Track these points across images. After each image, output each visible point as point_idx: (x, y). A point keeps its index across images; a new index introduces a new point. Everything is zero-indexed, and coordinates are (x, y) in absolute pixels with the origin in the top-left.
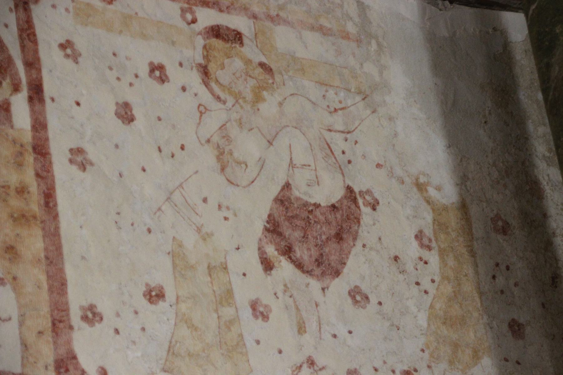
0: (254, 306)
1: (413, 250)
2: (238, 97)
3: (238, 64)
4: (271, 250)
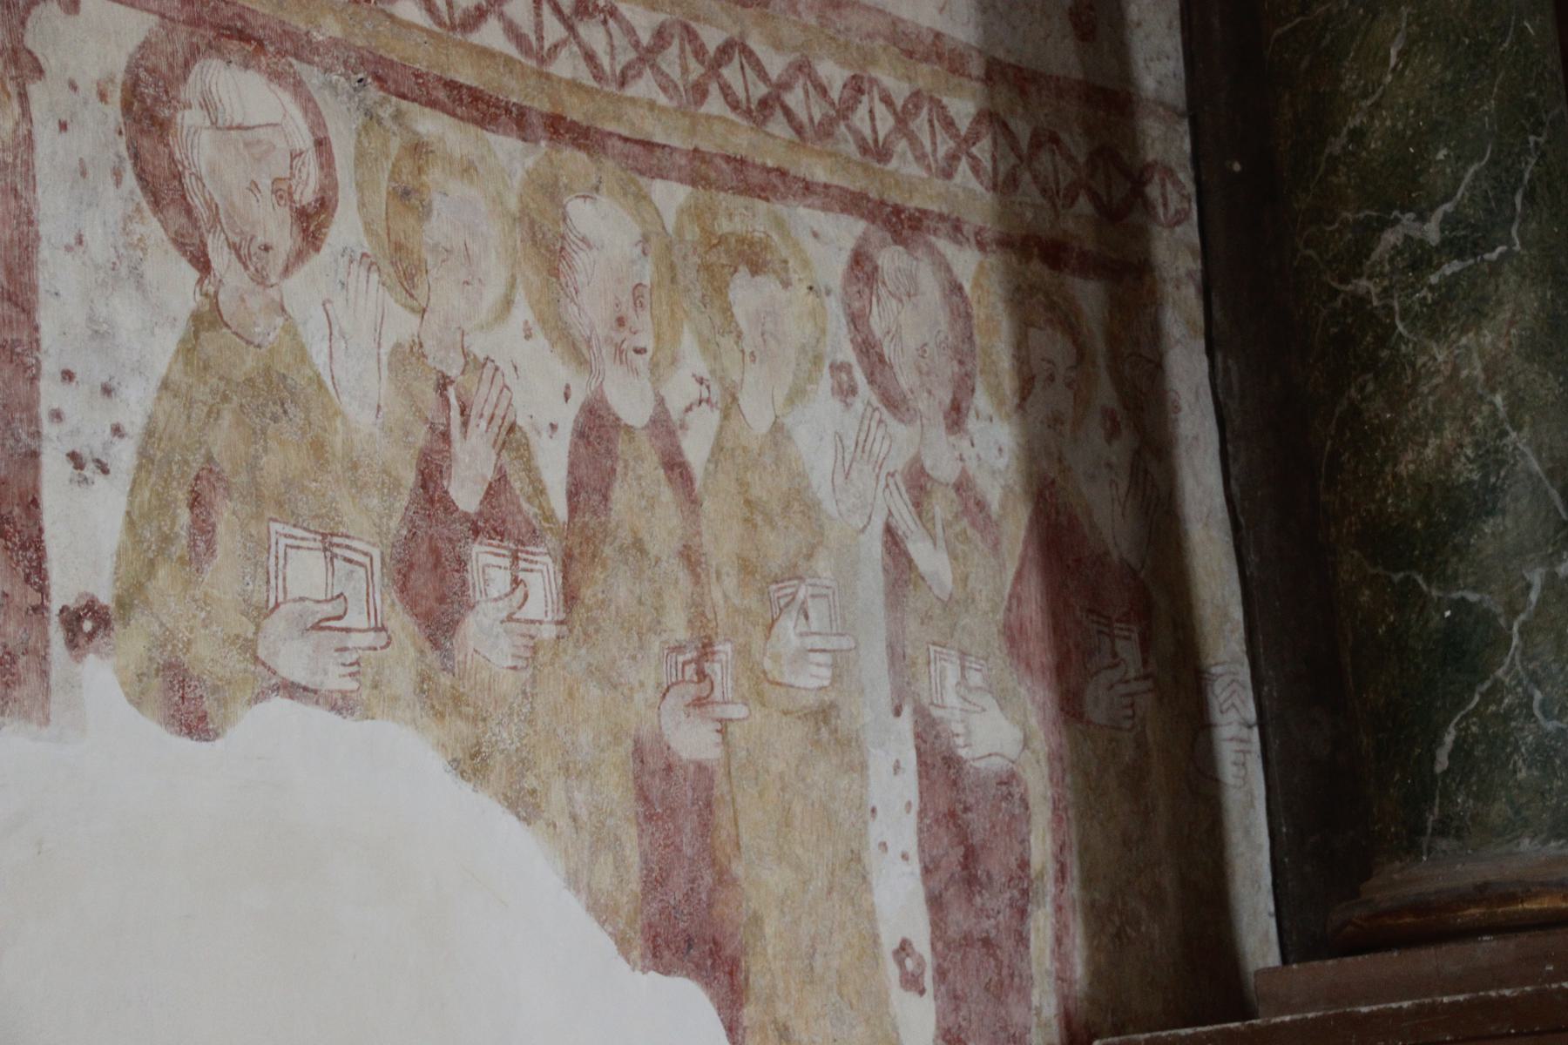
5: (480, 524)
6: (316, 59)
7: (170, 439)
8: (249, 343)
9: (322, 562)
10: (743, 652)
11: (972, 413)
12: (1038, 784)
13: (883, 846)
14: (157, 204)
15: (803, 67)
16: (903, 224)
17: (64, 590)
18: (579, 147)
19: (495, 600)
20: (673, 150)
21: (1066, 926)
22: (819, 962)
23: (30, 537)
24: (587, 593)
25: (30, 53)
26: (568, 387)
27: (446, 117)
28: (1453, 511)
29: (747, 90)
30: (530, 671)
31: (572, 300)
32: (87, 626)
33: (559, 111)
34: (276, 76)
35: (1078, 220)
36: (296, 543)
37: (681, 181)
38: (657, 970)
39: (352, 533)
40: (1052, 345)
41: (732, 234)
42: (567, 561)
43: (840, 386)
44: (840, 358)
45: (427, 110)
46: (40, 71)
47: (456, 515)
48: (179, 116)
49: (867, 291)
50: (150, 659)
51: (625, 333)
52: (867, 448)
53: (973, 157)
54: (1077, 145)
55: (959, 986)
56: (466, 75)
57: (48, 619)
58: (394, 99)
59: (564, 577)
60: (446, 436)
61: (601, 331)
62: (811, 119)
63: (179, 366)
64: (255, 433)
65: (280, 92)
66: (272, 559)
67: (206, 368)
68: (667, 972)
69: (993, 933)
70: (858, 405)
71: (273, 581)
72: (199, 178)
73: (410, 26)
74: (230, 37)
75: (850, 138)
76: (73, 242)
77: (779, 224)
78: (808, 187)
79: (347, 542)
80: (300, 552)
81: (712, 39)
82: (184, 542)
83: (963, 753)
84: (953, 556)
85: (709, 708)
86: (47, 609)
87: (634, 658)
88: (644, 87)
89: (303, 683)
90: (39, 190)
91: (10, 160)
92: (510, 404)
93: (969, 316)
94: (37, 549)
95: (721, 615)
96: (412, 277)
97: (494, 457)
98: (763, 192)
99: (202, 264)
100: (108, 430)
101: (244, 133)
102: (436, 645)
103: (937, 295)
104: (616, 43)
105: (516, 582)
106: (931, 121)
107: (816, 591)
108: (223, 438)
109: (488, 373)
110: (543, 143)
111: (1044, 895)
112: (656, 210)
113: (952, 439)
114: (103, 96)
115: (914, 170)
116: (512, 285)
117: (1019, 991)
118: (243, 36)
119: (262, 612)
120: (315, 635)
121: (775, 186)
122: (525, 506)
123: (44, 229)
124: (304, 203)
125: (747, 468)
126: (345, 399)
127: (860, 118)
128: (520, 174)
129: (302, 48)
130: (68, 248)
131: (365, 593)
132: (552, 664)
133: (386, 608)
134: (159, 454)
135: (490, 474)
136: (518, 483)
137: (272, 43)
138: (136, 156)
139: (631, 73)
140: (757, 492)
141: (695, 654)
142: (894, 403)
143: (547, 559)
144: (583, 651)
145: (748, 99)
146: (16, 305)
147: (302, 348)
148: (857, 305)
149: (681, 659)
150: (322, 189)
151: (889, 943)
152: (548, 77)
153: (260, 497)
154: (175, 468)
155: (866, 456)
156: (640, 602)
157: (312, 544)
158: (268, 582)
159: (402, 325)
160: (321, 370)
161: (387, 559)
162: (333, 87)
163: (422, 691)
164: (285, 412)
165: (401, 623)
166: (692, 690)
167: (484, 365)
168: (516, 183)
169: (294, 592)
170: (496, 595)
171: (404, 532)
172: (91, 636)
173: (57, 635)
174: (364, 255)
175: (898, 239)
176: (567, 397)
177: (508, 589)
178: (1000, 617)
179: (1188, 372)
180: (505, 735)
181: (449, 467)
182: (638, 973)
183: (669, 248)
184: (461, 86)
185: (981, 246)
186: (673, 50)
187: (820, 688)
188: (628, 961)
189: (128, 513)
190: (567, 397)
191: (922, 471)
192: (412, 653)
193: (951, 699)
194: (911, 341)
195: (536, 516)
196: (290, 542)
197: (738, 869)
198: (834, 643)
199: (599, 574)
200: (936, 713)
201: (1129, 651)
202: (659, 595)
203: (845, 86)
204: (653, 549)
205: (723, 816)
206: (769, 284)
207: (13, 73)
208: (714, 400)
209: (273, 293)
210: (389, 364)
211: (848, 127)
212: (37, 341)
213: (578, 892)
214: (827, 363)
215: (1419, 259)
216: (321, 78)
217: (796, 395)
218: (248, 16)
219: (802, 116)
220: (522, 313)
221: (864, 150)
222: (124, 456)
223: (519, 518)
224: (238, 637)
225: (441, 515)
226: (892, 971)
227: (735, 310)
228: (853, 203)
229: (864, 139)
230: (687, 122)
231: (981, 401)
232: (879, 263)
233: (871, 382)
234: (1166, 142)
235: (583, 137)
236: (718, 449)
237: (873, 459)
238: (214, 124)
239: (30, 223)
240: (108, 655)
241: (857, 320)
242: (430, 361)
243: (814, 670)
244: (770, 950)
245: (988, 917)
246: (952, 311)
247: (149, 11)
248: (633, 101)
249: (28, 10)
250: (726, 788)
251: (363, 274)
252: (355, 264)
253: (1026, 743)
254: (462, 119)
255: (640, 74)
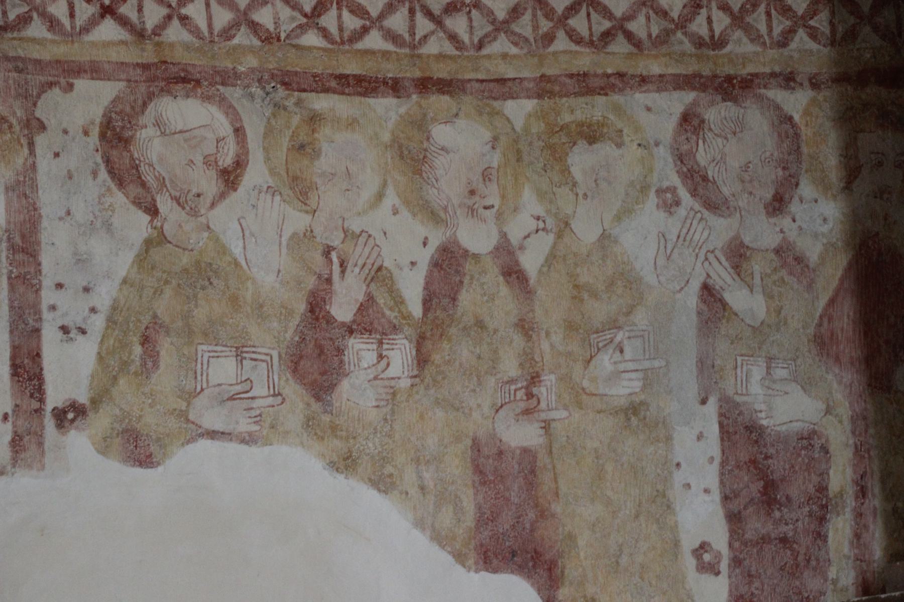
5: (354, 327)
6: (239, 82)
7: (128, 309)
8: (184, 249)
9: (234, 363)
10: (565, 379)
11: (796, 199)
13: (688, 486)
14: (121, 184)
17: (55, 397)
18: (444, 93)
19: (366, 369)
20: (521, 80)
21: (866, 527)
22: (624, 560)
23: (35, 374)
24: (436, 358)
25: (38, 119)
26: (426, 238)
27: (336, 97)
29: (590, 29)
30: (390, 407)
31: (433, 186)
32: (70, 416)
33: (427, 74)
34: (207, 98)
36: (216, 354)
37: (529, 97)
38: (487, 570)
39: (257, 344)
41: (573, 122)
42: (420, 342)
43: (665, 202)
44: (665, 184)
45: (322, 95)
46: (43, 127)
47: (335, 324)
48: (138, 133)
49: (694, 137)
50: (112, 429)
51: (477, 198)
52: (688, 239)
53: (811, 27)
55: (753, 569)
56: (352, 68)
57: (44, 415)
58: (296, 93)
59: (417, 350)
60: (329, 281)
61: (456, 201)
62: (650, 36)
63: (135, 269)
64: (188, 298)
65: (209, 107)
66: (199, 366)
67: (152, 268)
68: (495, 571)
69: (791, 534)
70: (682, 212)
71: (199, 378)
72: (151, 165)
73: (310, 49)
74: (176, 83)
75: (686, 40)
76: (63, 215)
77: (618, 109)
78: (644, 80)
79: (254, 349)
80: (219, 359)
82: (138, 364)
83: (764, 422)
84: (769, 296)
85: (536, 415)
86: (43, 410)
87: (474, 391)
89: (221, 430)
90: (40, 192)
91: (22, 179)
92: (379, 255)
93: (797, 135)
94: (39, 379)
95: (547, 357)
96: (306, 193)
97: (364, 288)
99: (153, 211)
100: (87, 310)
101: (184, 135)
102: (318, 398)
103: (766, 128)
104: (475, 24)
105: (381, 357)
106: (768, 14)
107: (632, 334)
108: (165, 305)
109: (362, 240)
110: (414, 97)
111: (844, 507)
112: (508, 119)
113: (772, 220)
114: (86, 133)
115: (749, 48)
116: (385, 185)
117: (815, 569)
118: (185, 80)
119: (191, 396)
120: (230, 403)
121: (613, 85)
122: (388, 313)
123: (43, 212)
124: (225, 166)
125: (576, 265)
126: (254, 270)
127: (699, 26)
128: (394, 117)
129: (227, 78)
130: (61, 219)
131: (265, 376)
132: (408, 401)
133: (282, 383)
134: (121, 319)
135: (361, 298)
136: (382, 299)
137: (206, 80)
138: (108, 161)
139: (486, 40)
140: (585, 277)
141: (525, 384)
143: (405, 342)
144: (432, 391)
145: (591, 35)
146: (27, 254)
147: (223, 246)
148: (685, 148)
149: (513, 387)
150: (238, 156)
151: (688, 543)
152: (419, 56)
153: (191, 333)
154: (131, 325)
155: (687, 243)
156: (479, 357)
157: (228, 354)
158: (196, 378)
159: (298, 221)
160: (237, 256)
161: (284, 356)
162: (252, 96)
163: (308, 426)
164: (211, 283)
165: (293, 390)
166: (522, 405)
167: (360, 235)
168: (390, 125)
169: (214, 380)
170: (366, 366)
171: (297, 339)
172: (73, 421)
173: (49, 423)
174: (269, 187)
175: (728, 96)
176: (425, 244)
177: (375, 361)
178: (811, 331)
180: (371, 445)
181: (331, 298)
182: (472, 574)
183: (516, 141)
184: (348, 76)
185: (815, 85)
186: (528, 16)
187: (631, 394)
188: (464, 566)
189: (99, 353)
190: (425, 244)
191: (742, 245)
192: (301, 405)
193: (756, 388)
194: (735, 163)
195: (396, 317)
196: (212, 354)
197: (557, 508)
198: (647, 364)
199: (445, 345)
200: (738, 399)
202: (496, 352)
203: (684, 7)
204: (491, 325)
205: (546, 478)
206: (605, 149)
207: (26, 132)
208: (549, 227)
209: (203, 220)
210: (288, 245)
211: (685, 34)
212: (40, 271)
213: (423, 529)
214: (653, 190)
216: (241, 92)
218: (190, 69)
219: (642, 34)
220: (391, 199)
221: (699, 43)
222: (98, 323)
223: (383, 320)
224: (175, 410)
225: (324, 325)
226: (690, 562)
227: (572, 169)
229: (700, 37)
230: (536, 59)
232: (706, 117)
233: (694, 193)
235: (446, 86)
236: (551, 258)
237: (694, 244)
238: (163, 134)
239: (35, 209)
240: (84, 430)
242: (318, 239)
243: (625, 383)
244: (582, 554)
245: (787, 524)
246: (779, 135)
247: (119, 80)
248: (489, 57)
249: (39, 96)
250: (548, 461)
251: (269, 197)
252: (263, 194)
253: (828, 411)
254: (348, 95)
255: (495, 39)
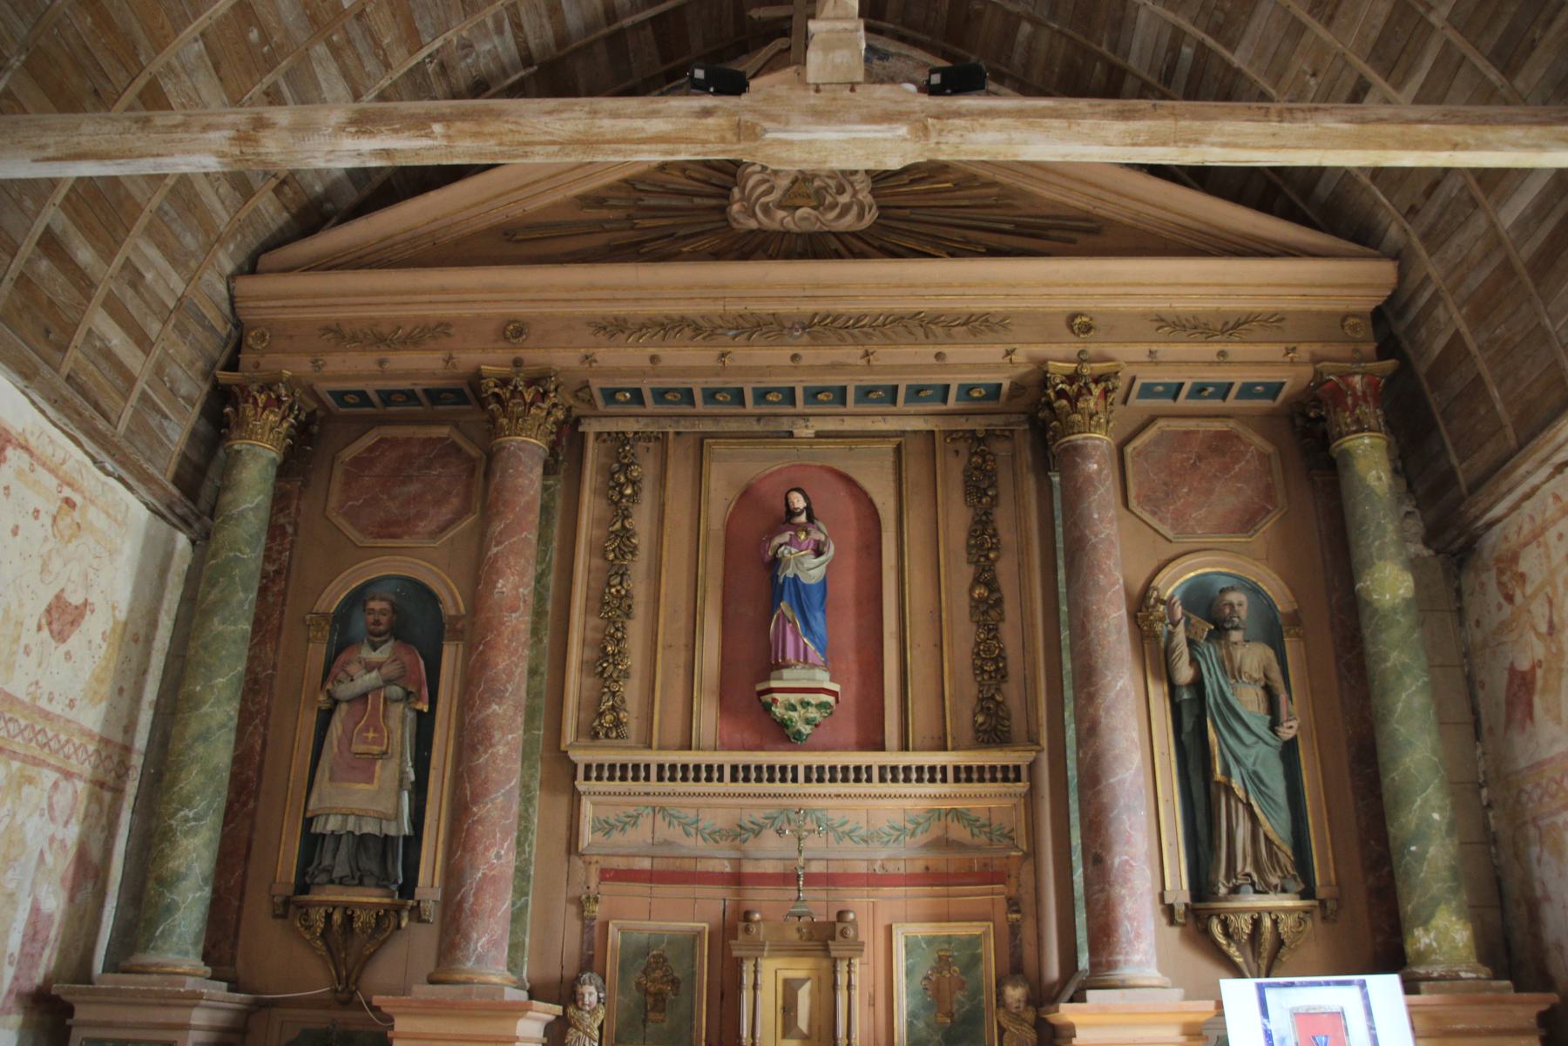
0: (26, 647)
1: (98, 639)
2: (62, 536)
3: (69, 520)
4: (44, 621)
12: (58, 918)
15: (57, 736)
16: (68, 775)
28: (179, 877)
35: (110, 779)
40: (95, 808)
54: (116, 759)
81: (38, 728)
88: (19, 739)
98: (38, 765)
142: (52, 819)
179: (126, 817)
201: (90, 886)
215: (186, 820)
217: (30, 815)
228: (58, 769)
231: (73, 820)
234: (137, 760)
241: (50, 798)
